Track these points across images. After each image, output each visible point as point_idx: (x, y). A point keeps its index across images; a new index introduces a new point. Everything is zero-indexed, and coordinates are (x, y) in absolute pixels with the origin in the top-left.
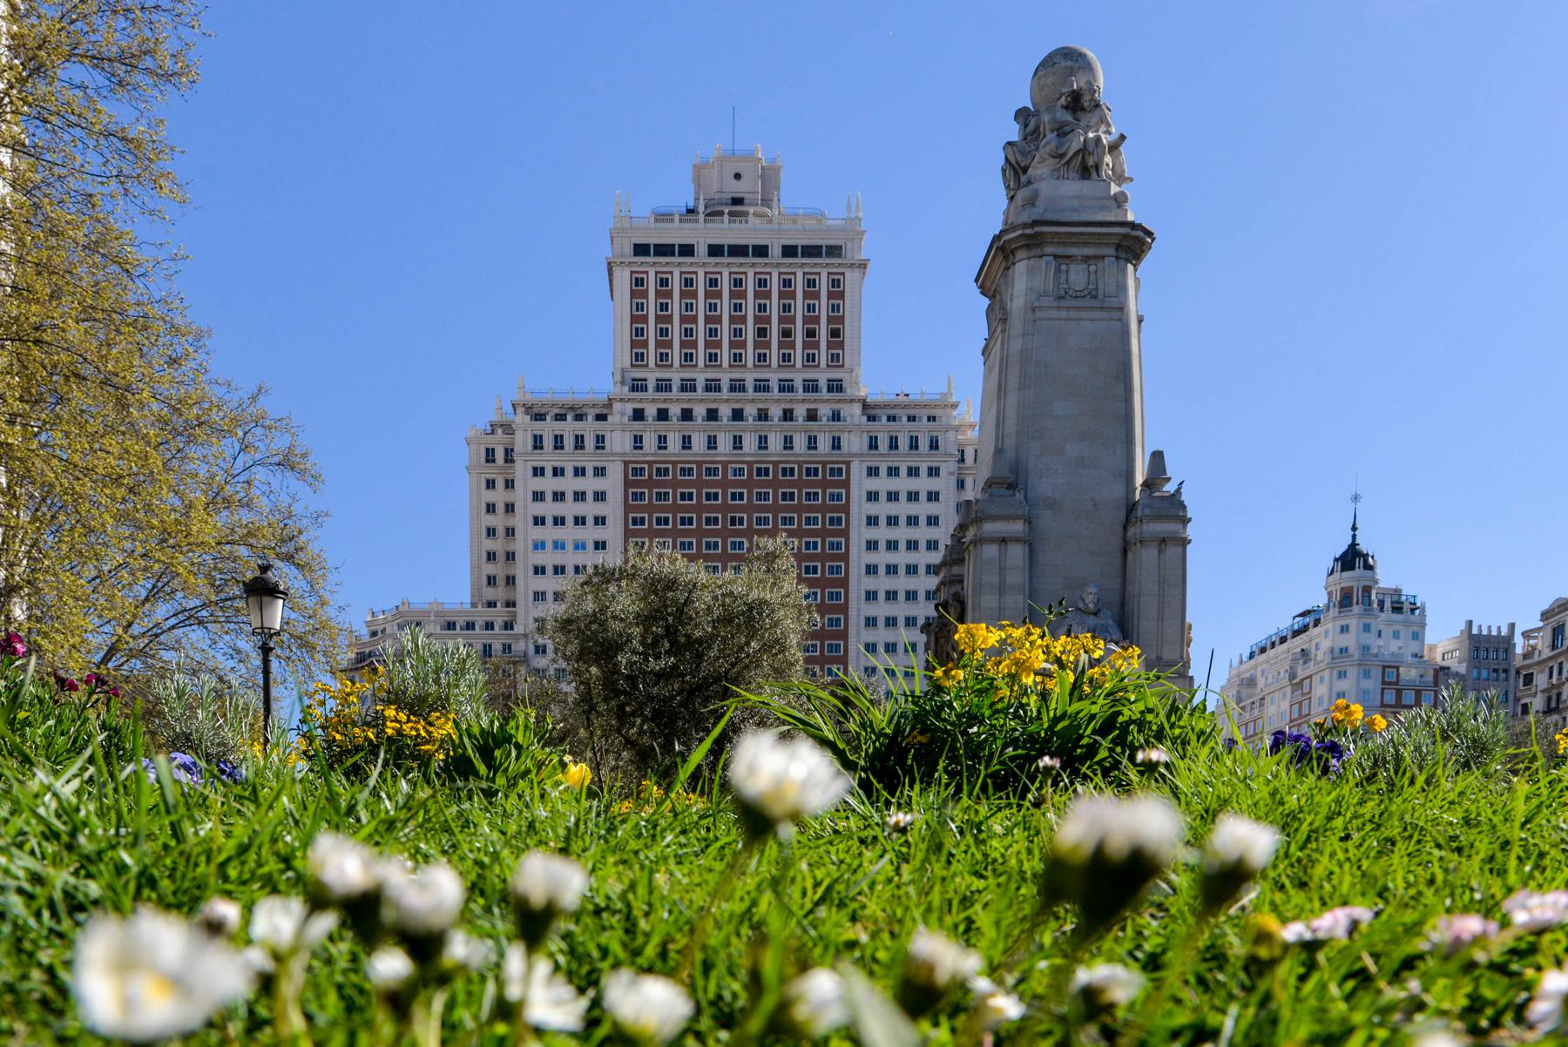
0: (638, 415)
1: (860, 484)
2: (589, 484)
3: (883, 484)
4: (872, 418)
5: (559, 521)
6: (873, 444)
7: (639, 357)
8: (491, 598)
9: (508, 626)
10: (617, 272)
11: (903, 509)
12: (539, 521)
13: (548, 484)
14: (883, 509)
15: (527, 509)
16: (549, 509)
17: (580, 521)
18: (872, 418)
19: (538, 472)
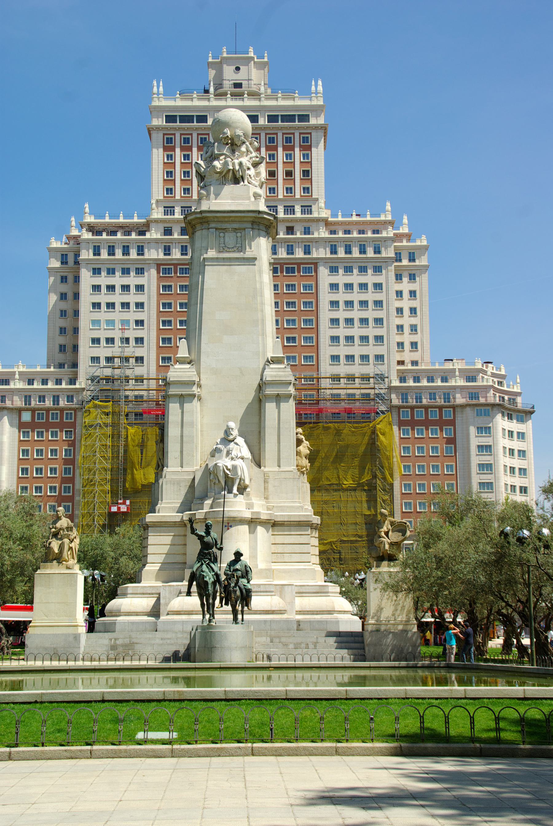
0: (168, 231)
1: (325, 277)
2: (132, 280)
3: (341, 278)
4: (333, 232)
5: (111, 305)
6: (334, 251)
7: (170, 191)
8: (61, 361)
9: (73, 381)
10: (154, 135)
11: (356, 296)
12: (96, 305)
13: (103, 280)
14: (342, 296)
15: (87, 297)
16: (103, 298)
17: (125, 305)
18: (333, 232)
19: (96, 271)
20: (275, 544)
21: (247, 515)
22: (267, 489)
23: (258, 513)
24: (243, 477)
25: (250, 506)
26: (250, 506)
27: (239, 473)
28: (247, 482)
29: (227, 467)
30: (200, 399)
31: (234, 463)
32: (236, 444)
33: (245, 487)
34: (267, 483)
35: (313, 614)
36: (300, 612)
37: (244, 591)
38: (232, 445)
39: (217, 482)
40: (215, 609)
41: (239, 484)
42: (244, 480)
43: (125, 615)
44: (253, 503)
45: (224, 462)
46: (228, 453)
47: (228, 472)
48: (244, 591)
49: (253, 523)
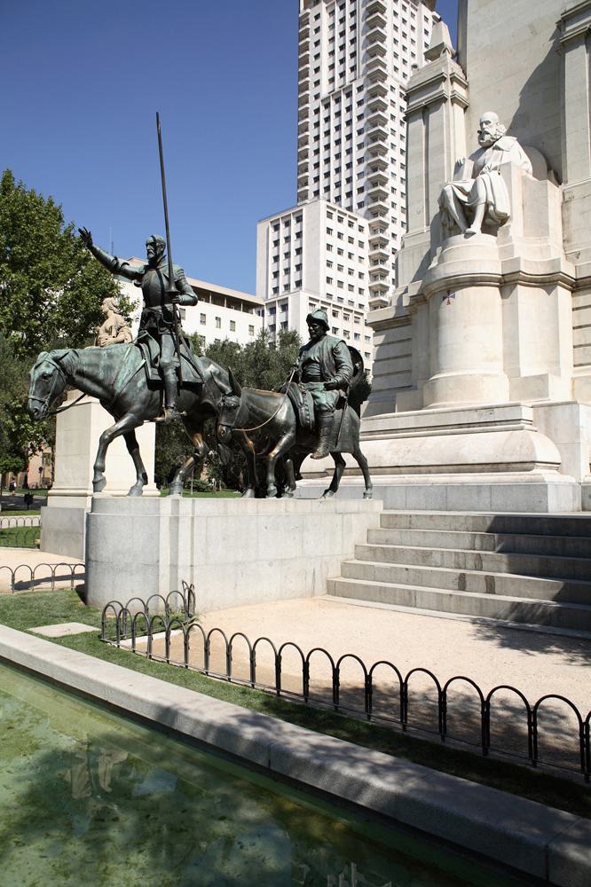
20: (580, 327)
21: (495, 268)
22: (568, 222)
23: (517, 261)
25: (507, 250)
26: (507, 250)
28: (502, 208)
29: (462, 190)
30: (454, 100)
32: (498, 148)
33: (504, 219)
34: (568, 209)
39: (452, 224)
41: (487, 213)
42: (494, 206)
44: (513, 246)
47: (465, 198)
48: (308, 413)
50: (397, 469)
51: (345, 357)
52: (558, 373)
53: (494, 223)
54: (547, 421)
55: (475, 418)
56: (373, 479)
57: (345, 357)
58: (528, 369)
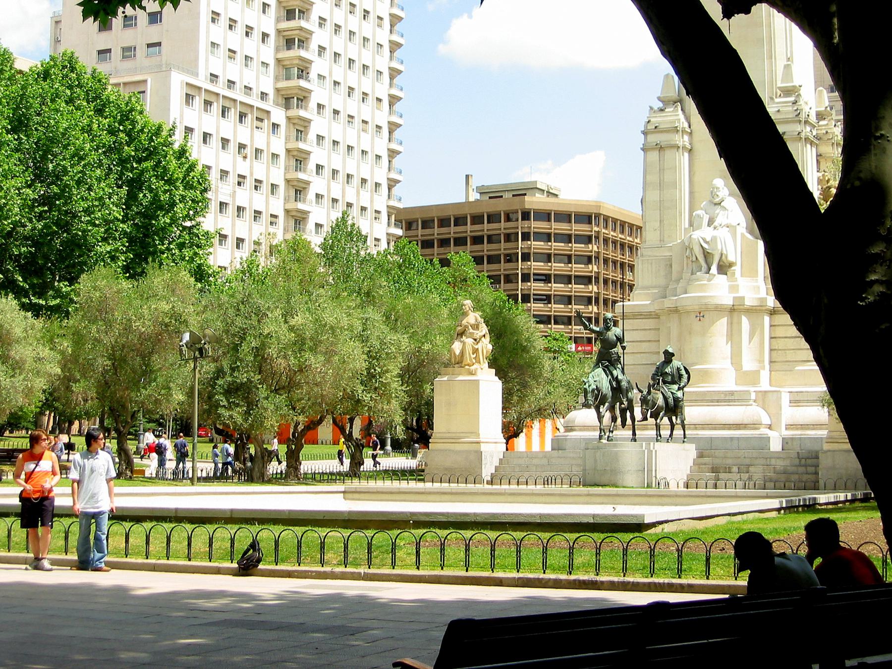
21: (727, 300)
23: (743, 298)
24: (724, 252)
25: (733, 288)
26: (733, 288)
27: (719, 247)
28: (731, 258)
29: (704, 240)
31: (715, 233)
32: (725, 209)
33: (731, 265)
35: (715, 429)
36: (789, 427)
37: (671, 401)
38: (718, 210)
39: (694, 259)
40: (636, 423)
43: (580, 430)
45: (704, 233)
46: (711, 222)
48: (671, 401)
49: (734, 310)
50: (696, 426)
51: (683, 372)
52: (764, 369)
53: (724, 268)
54: (763, 401)
55: (722, 397)
56: (687, 432)
57: (683, 372)
58: (748, 364)
